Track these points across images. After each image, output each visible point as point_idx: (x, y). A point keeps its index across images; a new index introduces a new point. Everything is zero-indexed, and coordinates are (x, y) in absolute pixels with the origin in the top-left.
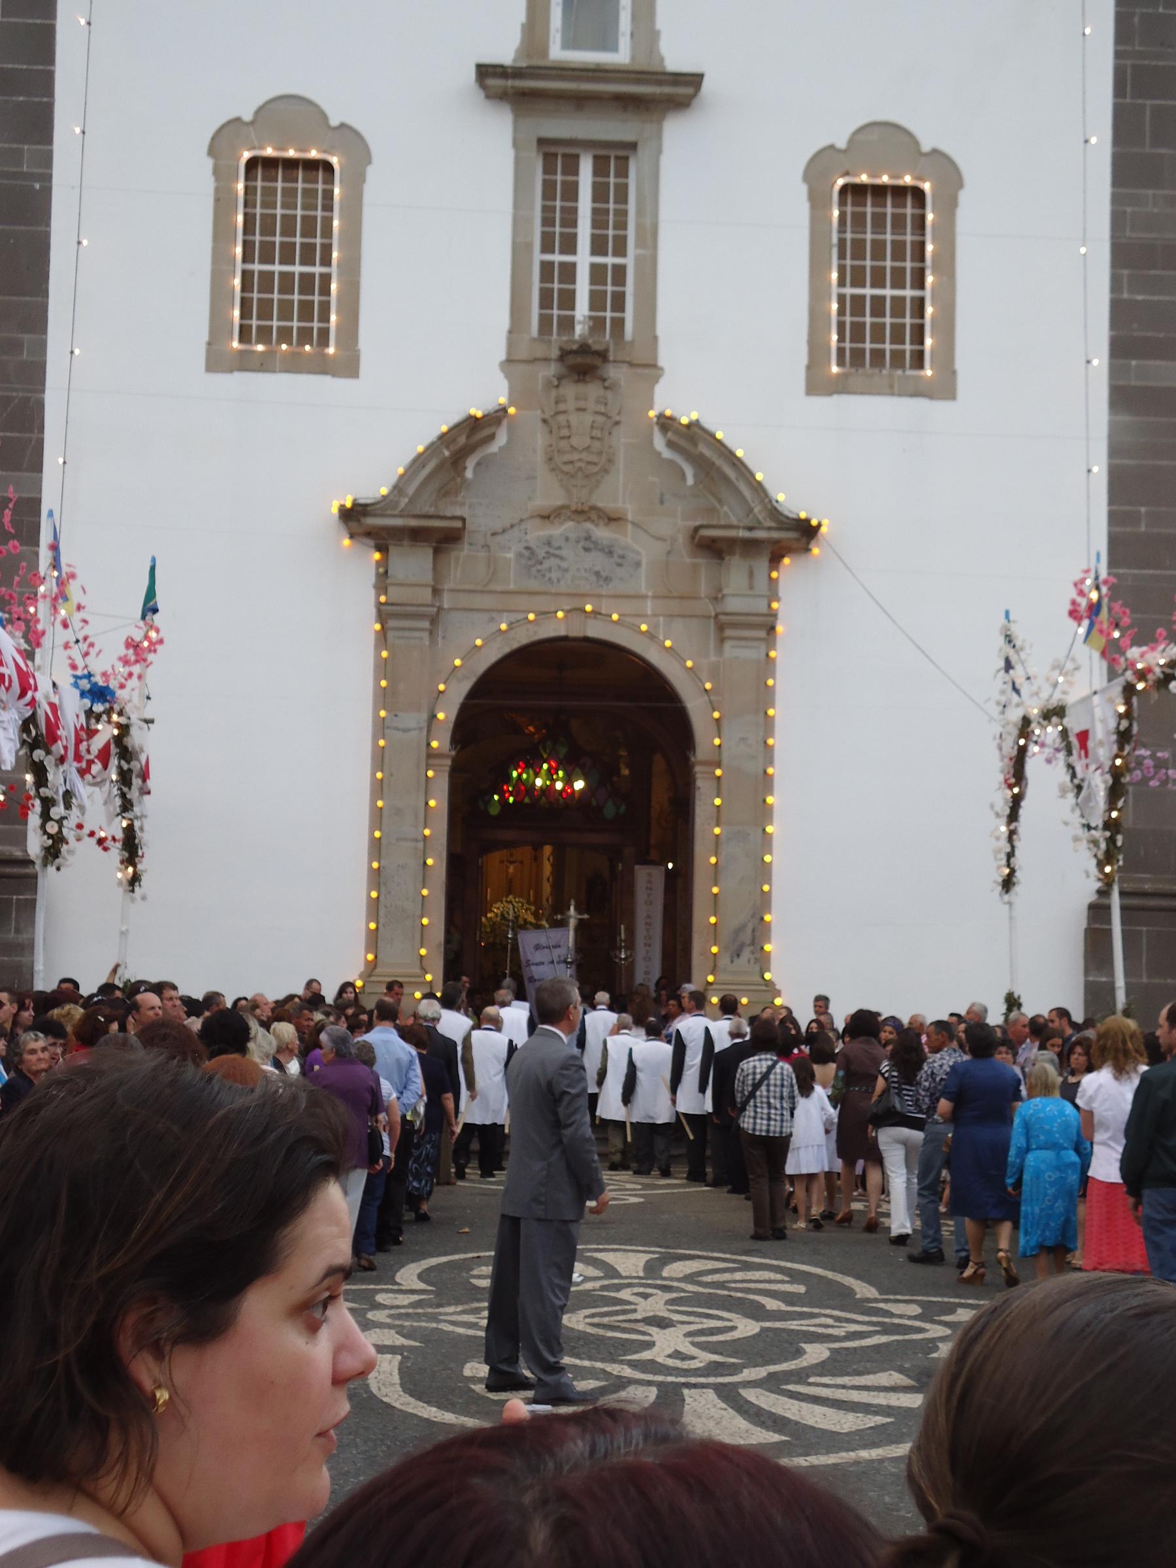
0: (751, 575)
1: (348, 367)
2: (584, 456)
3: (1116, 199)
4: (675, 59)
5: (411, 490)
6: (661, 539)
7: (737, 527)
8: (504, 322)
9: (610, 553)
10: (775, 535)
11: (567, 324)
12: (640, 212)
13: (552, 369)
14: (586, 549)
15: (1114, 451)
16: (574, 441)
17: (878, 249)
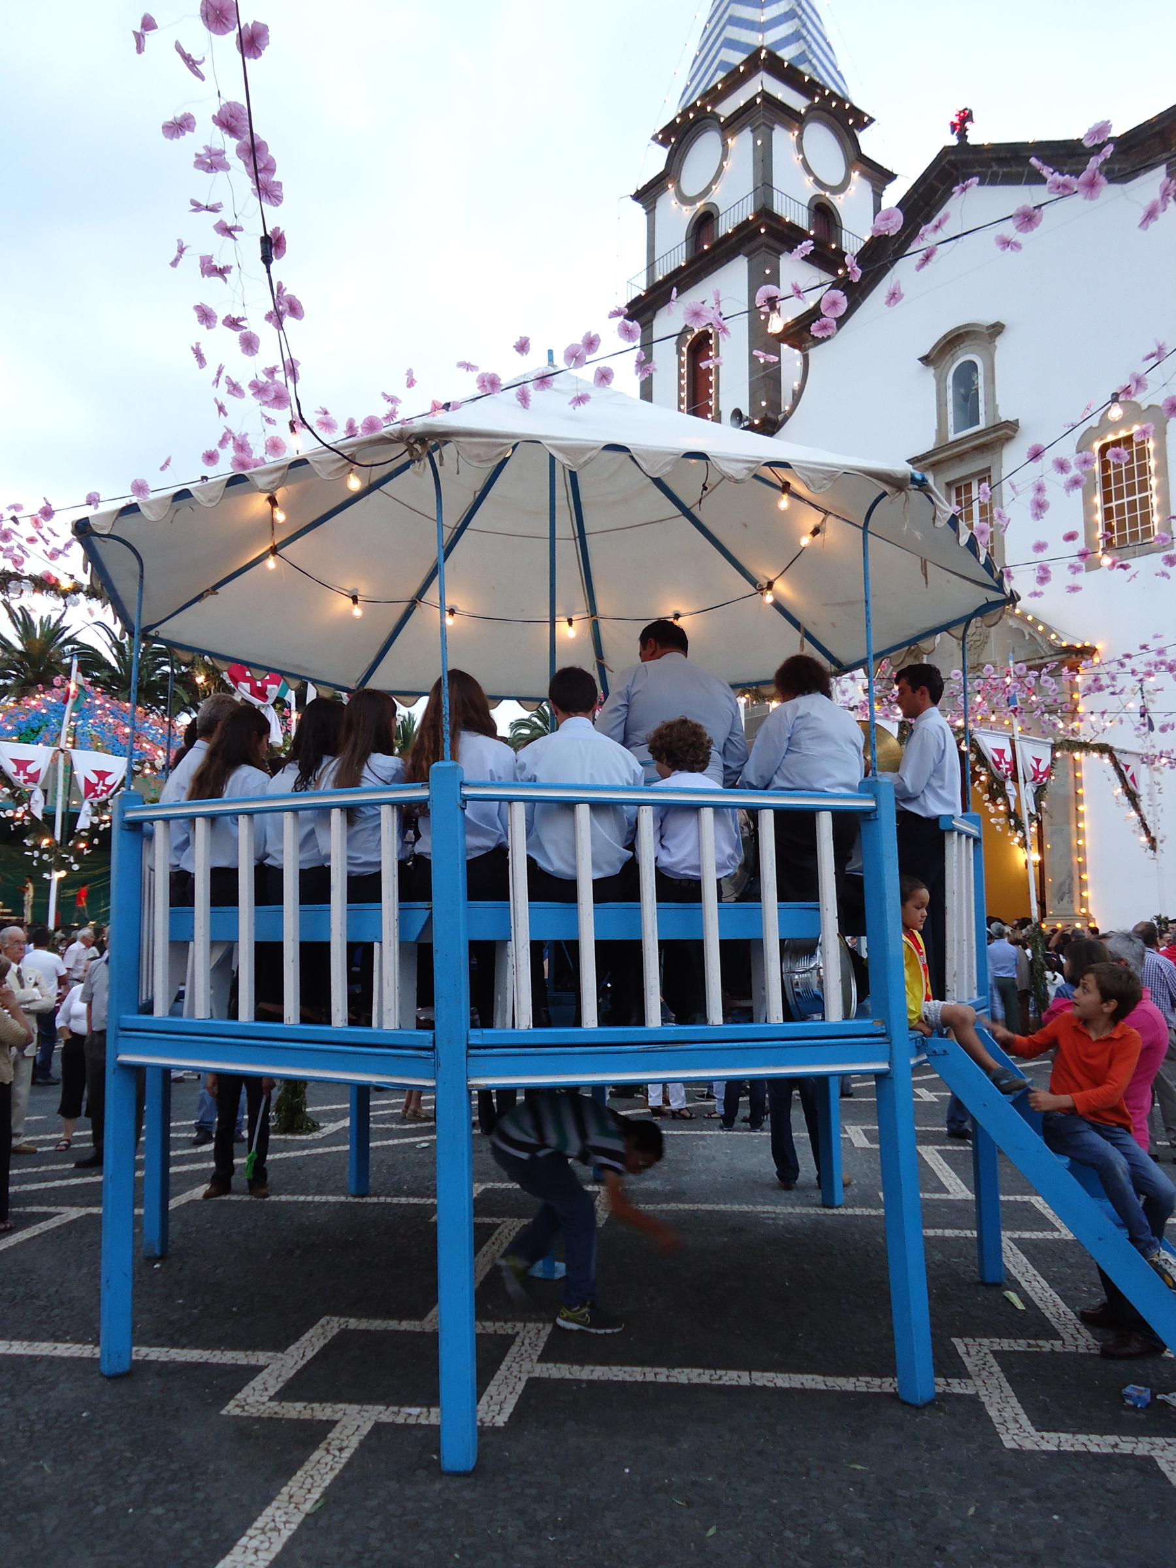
4: (1005, 415)
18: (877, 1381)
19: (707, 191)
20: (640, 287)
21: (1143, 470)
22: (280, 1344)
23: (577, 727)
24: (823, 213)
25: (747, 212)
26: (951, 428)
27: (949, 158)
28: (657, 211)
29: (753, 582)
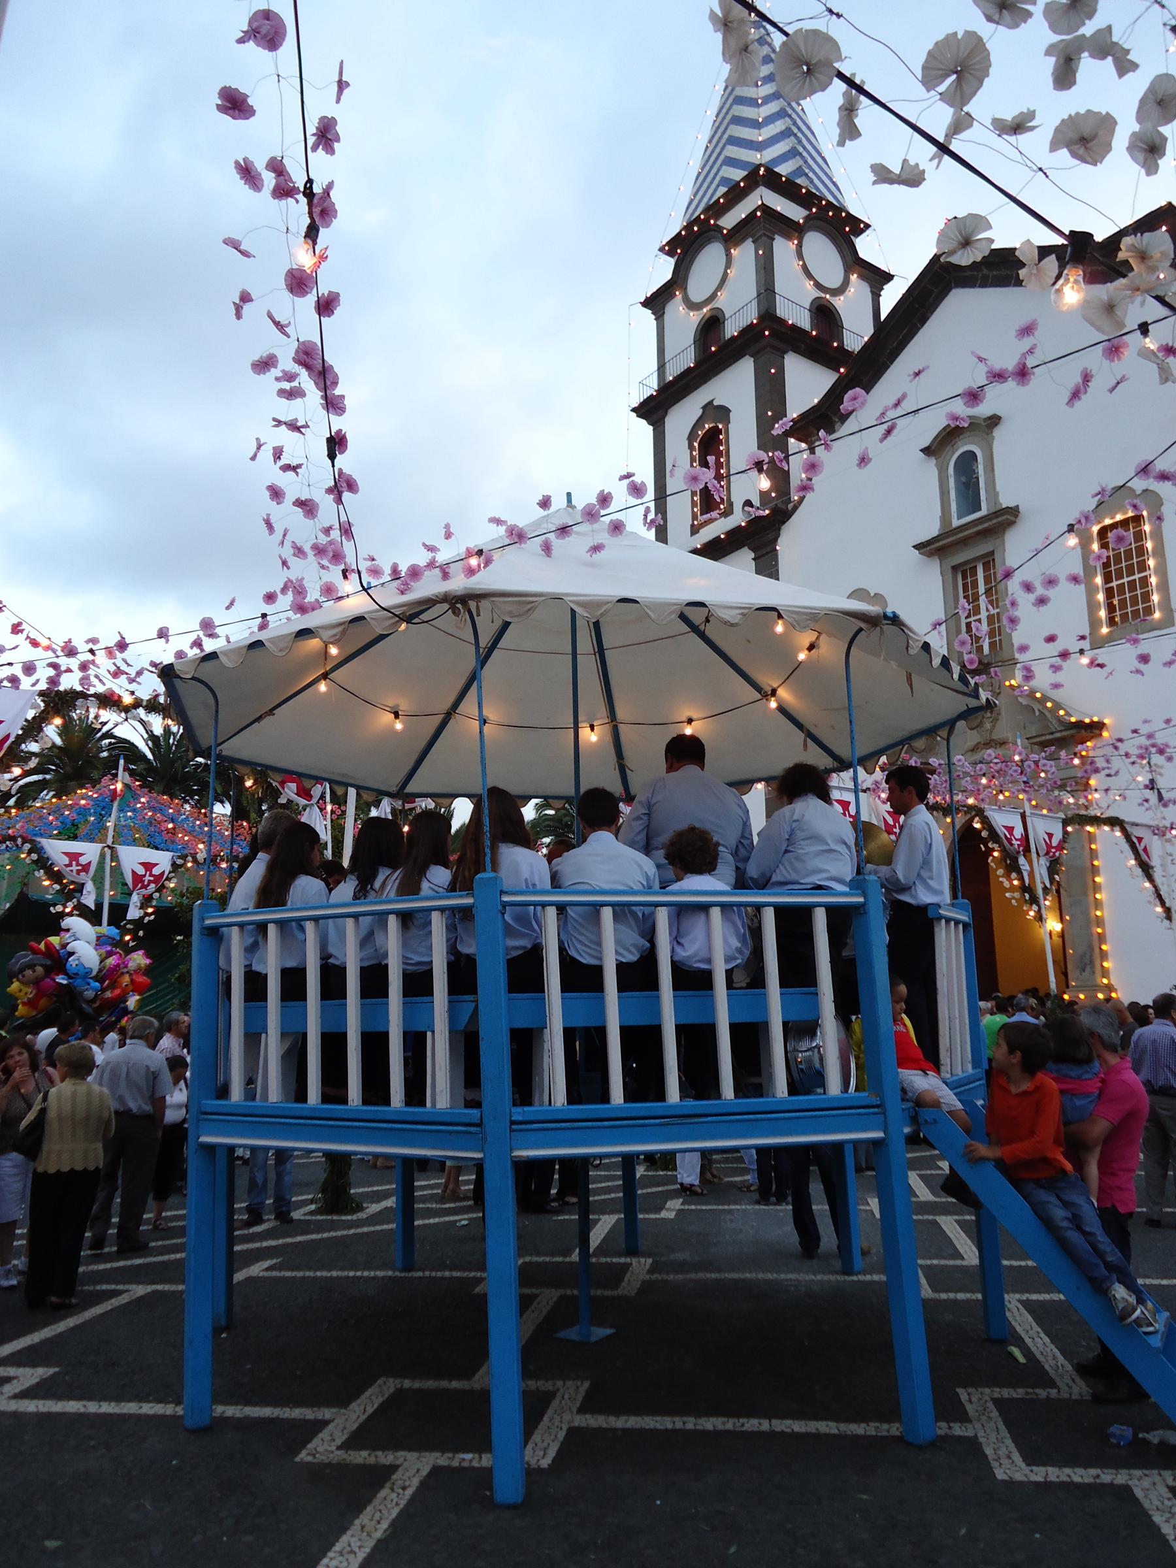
4: (1006, 501)
7: (1045, 735)
10: (1065, 733)
17: (1128, 553)
18: (885, 1426)
19: (713, 296)
20: (652, 386)
21: (1141, 551)
22: (343, 1400)
23: (602, 840)
24: (824, 314)
25: (751, 316)
26: (954, 515)
28: (665, 316)
29: (758, 689)
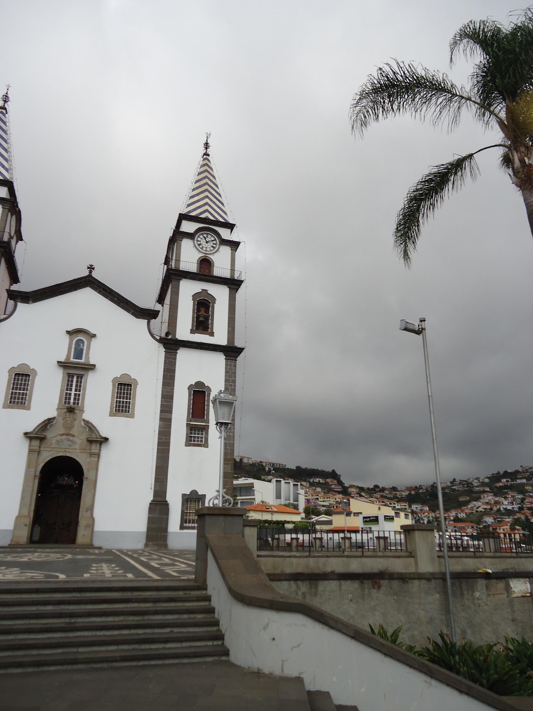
0: (96, 446)
1: (28, 408)
2: (70, 425)
3: (162, 388)
5: (37, 430)
6: (81, 439)
8: (57, 402)
9: (72, 442)
11: (69, 403)
12: (83, 386)
13: (66, 410)
14: (68, 441)
15: (160, 428)
16: (68, 423)
27: (90, 278)
